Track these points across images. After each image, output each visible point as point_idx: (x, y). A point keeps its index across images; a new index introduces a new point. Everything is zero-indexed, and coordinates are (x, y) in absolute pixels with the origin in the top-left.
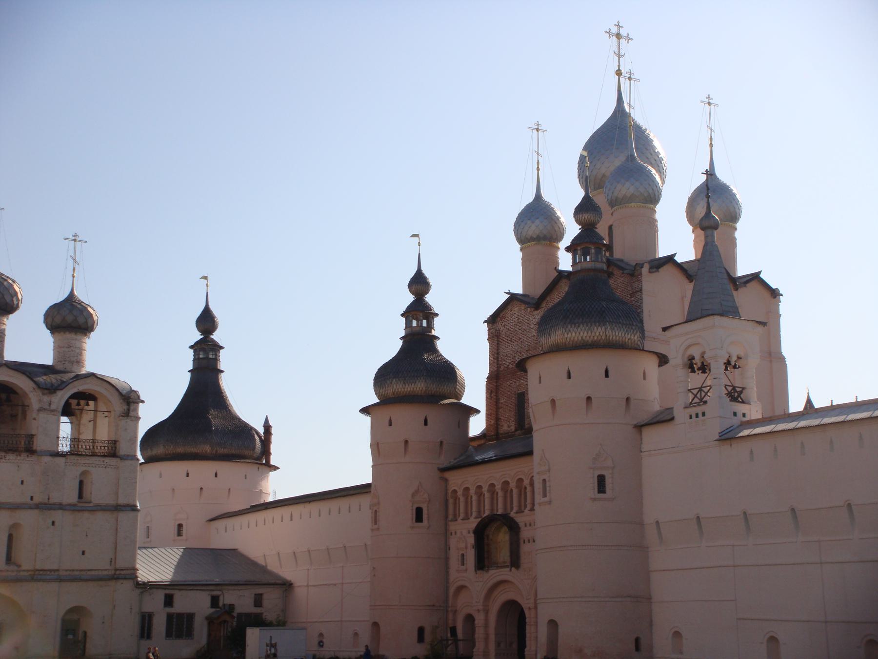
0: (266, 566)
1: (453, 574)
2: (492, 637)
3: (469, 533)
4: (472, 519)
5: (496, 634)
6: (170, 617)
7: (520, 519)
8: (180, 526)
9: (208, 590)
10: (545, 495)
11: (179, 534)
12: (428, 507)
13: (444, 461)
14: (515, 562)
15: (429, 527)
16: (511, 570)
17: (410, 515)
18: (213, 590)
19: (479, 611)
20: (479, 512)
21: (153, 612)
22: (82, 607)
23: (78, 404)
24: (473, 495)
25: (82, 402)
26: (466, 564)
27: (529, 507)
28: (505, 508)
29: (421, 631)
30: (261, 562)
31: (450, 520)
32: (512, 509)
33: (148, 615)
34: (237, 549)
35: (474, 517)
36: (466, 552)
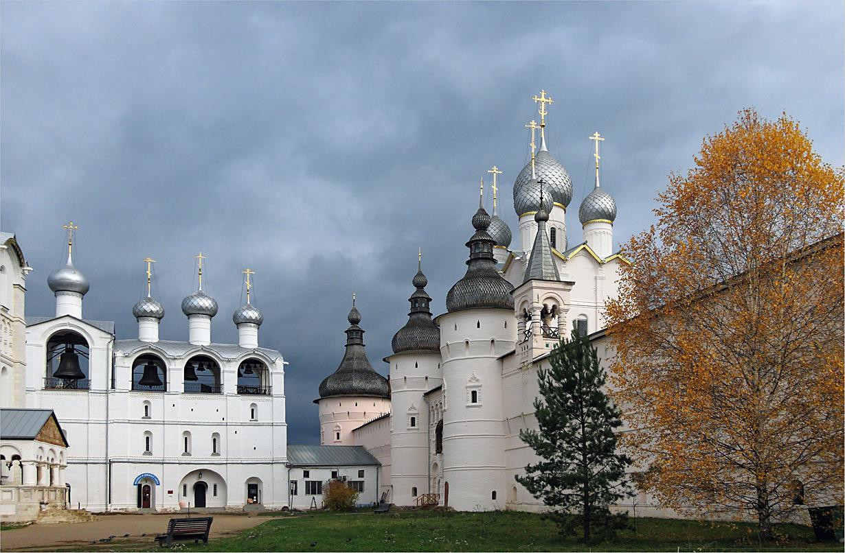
23: (255, 367)
25: (258, 365)
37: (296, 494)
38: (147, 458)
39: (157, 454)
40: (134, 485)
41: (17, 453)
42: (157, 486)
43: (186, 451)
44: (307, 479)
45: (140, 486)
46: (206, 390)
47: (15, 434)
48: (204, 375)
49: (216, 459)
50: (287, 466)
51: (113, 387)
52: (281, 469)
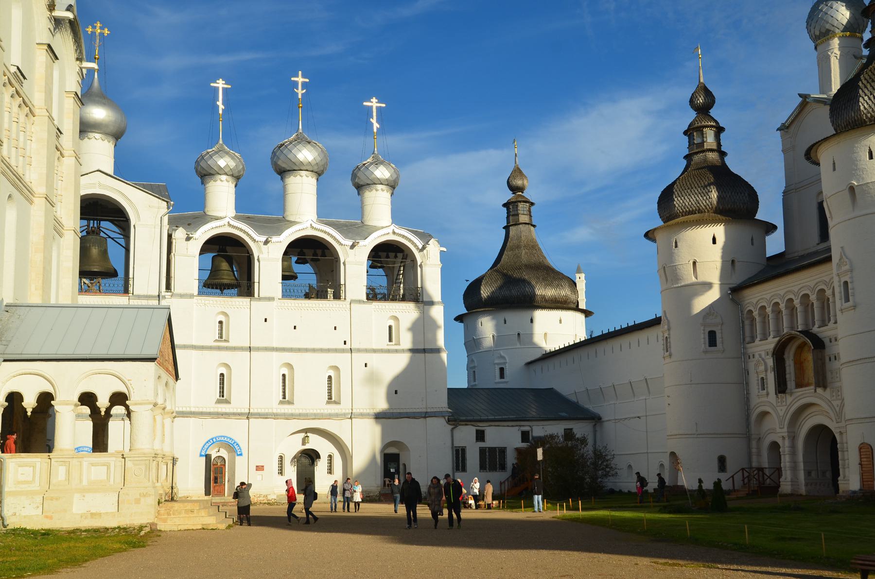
0: (578, 402)
1: (755, 400)
2: (801, 466)
3: (768, 355)
4: (770, 339)
5: (804, 462)
6: (482, 451)
7: (824, 333)
8: (502, 370)
9: (517, 426)
10: (847, 300)
11: (502, 375)
12: (721, 329)
13: (736, 280)
14: (822, 381)
15: (724, 351)
16: (815, 390)
17: (703, 338)
18: (523, 426)
19: (783, 438)
20: (778, 331)
21: (465, 447)
22: (402, 443)
24: (770, 313)
25: (392, 255)
26: (767, 387)
27: (832, 321)
28: (806, 324)
29: (722, 461)
30: (574, 399)
31: (747, 342)
32: (814, 324)
33: (461, 449)
34: (552, 388)
35: (773, 337)
36: (766, 375)
37: (464, 469)
38: (223, 408)
39: (238, 402)
40: (201, 455)
41: (122, 389)
42: (237, 458)
43: (284, 398)
44: (482, 444)
45: (208, 457)
46: (317, 293)
47: (113, 353)
48: (307, 274)
49: (333, 409)
50: (449, 421)
51: (168, 287)
52: (439, 426)
